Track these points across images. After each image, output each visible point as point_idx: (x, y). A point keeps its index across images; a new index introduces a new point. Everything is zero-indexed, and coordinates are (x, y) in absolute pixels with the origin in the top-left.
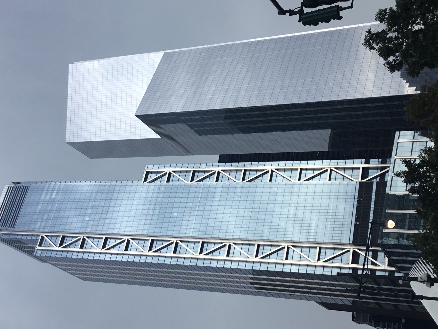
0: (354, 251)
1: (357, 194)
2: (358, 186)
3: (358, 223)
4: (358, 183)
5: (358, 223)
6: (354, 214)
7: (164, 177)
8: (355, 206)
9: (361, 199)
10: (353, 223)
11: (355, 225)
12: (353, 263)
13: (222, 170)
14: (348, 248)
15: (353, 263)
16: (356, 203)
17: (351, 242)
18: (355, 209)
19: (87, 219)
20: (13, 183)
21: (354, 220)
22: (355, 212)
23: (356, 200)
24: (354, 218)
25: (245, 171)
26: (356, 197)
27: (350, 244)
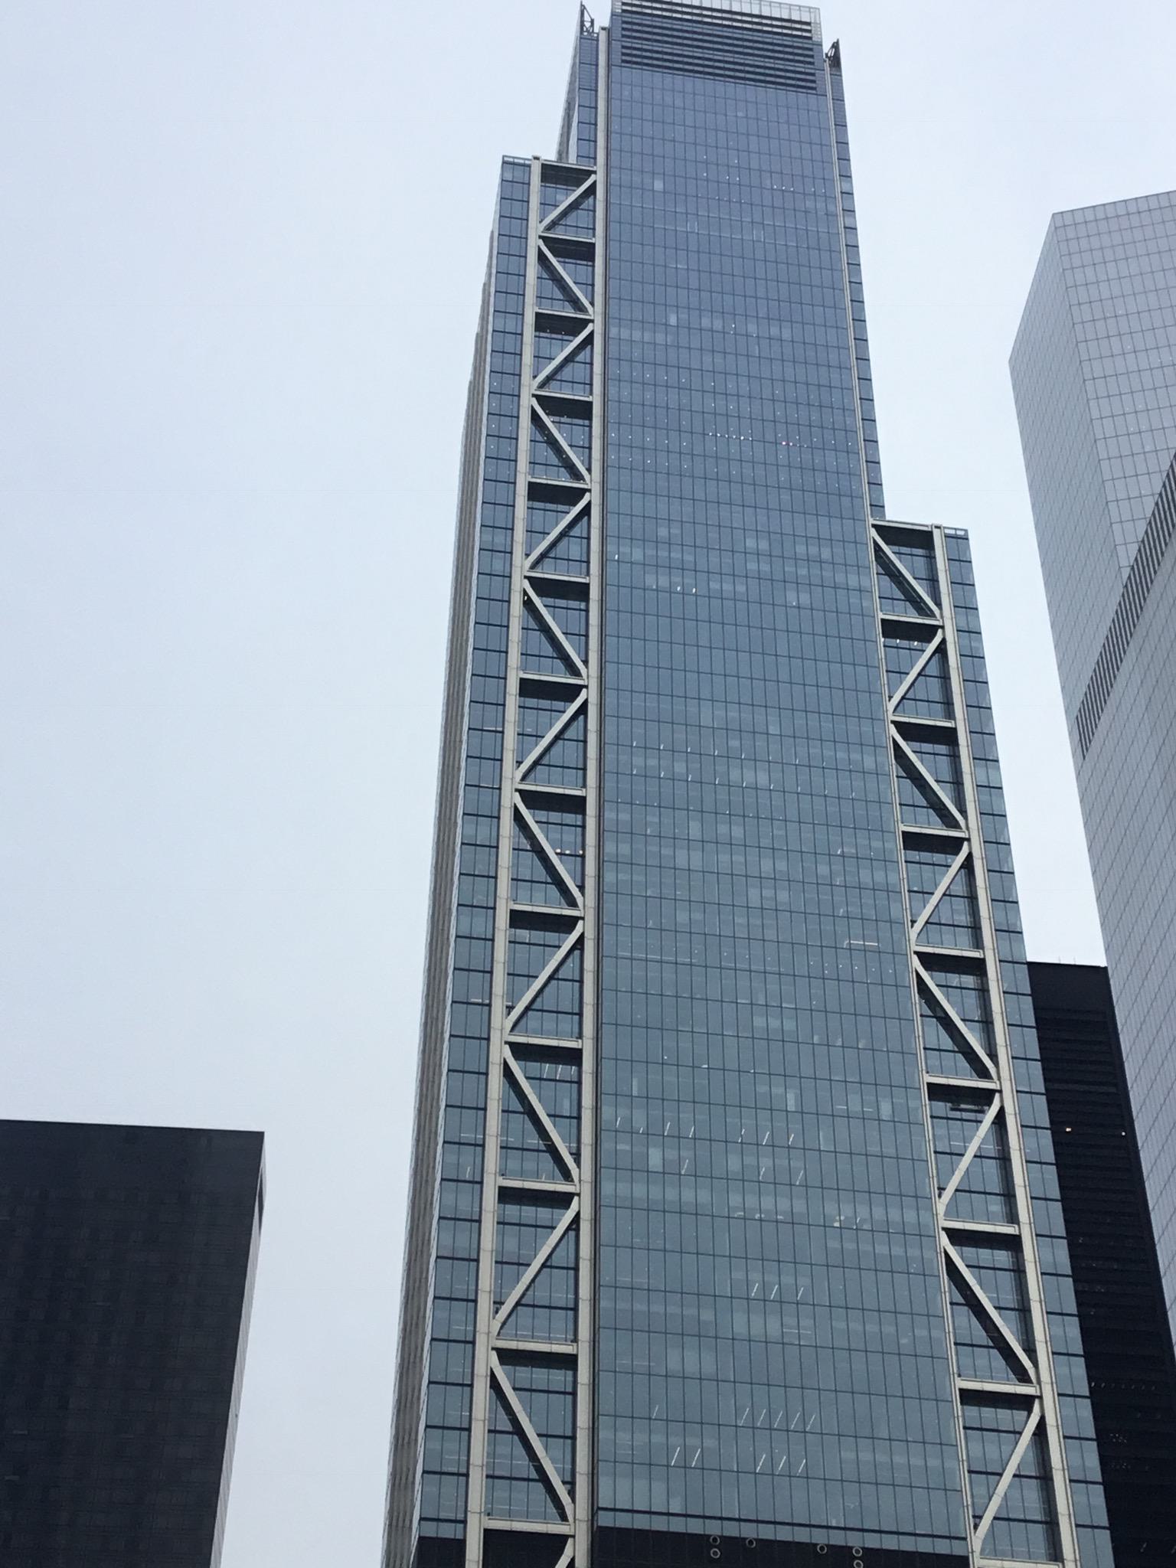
1: (890, 1543)
2: (942, 1547)
4: (957, 1549)
6: (767, 1533)
7: (934, 818)
13: (1001, 1112)
14: (579, 1509)
15: (488, 1532)
17: (605, 1520)
19: (673, 321)
20: (836, 46)
21: (731, 1530)
25: (1013, 1243)
27: (595, 1510)
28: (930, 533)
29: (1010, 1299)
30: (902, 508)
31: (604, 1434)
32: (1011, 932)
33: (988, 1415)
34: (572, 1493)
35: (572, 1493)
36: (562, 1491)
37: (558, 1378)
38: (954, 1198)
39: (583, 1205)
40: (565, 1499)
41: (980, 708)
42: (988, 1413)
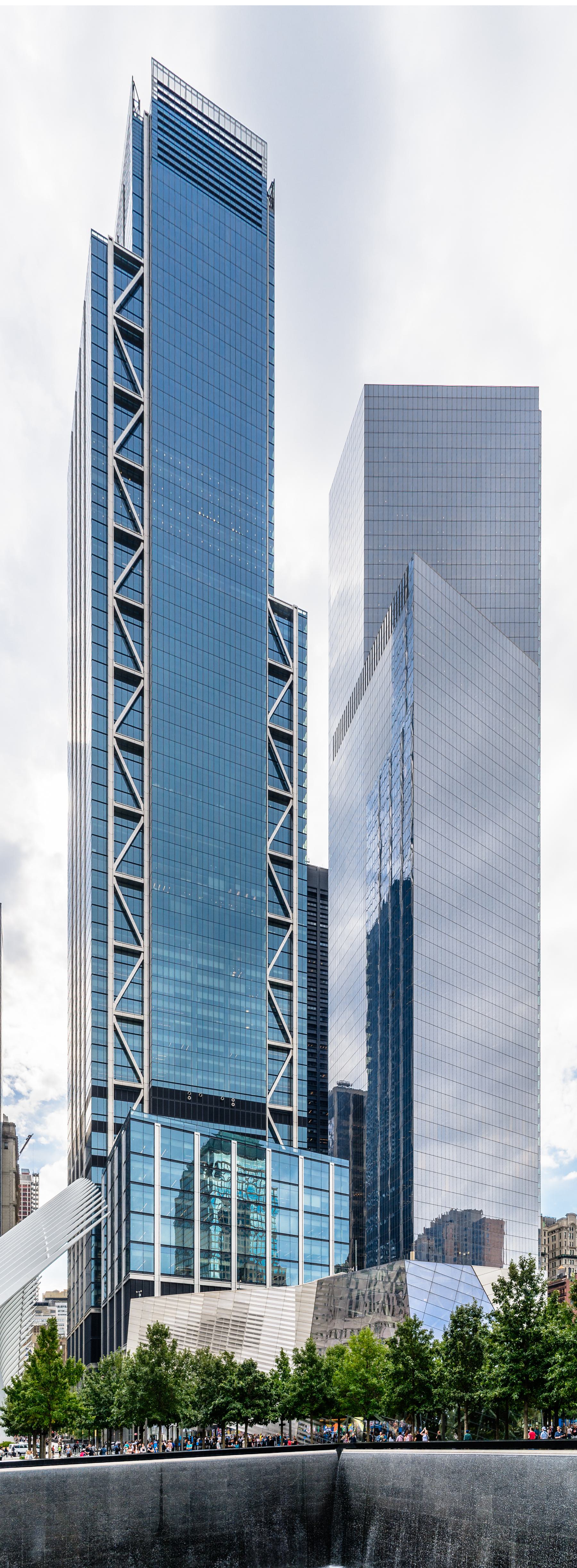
0: (140, 1090)
2: (259, 1100)
3: (190, 1098)
5: (190, 1098)
8: (222, 1095)
9: (233, 1105)
10: (189, 1090)
11: (184, 1094)
12: (117, 1088)
14: (145, 1079)
15: (117, 1088)
16: (227, 1095)
18: (216, 1094)
21: (195, 1090)
22: (211, 1093)
23: (233, 1097)
24: (200, 1091)
26: (238, 1097)
28: (292, 611)
29: (286, 1011)
30: (283, 593)
31: (154, 1052)
32: (303, 851)
33: (276, 1054)
34: (142, 1073)
35: (142, 1073)
36: (139, 1072)
37: (137, 1028)
38: (273, 969)
39: (145, 957)
40: (140, 1075)
41: (303, 728)
42: (276, 1053)
